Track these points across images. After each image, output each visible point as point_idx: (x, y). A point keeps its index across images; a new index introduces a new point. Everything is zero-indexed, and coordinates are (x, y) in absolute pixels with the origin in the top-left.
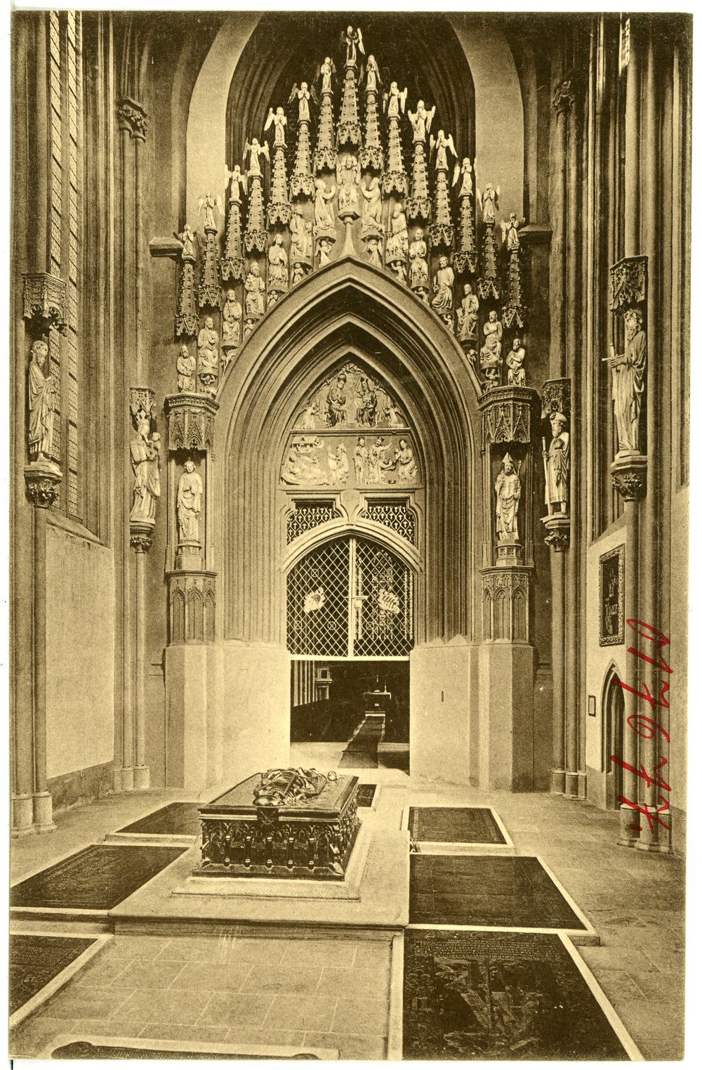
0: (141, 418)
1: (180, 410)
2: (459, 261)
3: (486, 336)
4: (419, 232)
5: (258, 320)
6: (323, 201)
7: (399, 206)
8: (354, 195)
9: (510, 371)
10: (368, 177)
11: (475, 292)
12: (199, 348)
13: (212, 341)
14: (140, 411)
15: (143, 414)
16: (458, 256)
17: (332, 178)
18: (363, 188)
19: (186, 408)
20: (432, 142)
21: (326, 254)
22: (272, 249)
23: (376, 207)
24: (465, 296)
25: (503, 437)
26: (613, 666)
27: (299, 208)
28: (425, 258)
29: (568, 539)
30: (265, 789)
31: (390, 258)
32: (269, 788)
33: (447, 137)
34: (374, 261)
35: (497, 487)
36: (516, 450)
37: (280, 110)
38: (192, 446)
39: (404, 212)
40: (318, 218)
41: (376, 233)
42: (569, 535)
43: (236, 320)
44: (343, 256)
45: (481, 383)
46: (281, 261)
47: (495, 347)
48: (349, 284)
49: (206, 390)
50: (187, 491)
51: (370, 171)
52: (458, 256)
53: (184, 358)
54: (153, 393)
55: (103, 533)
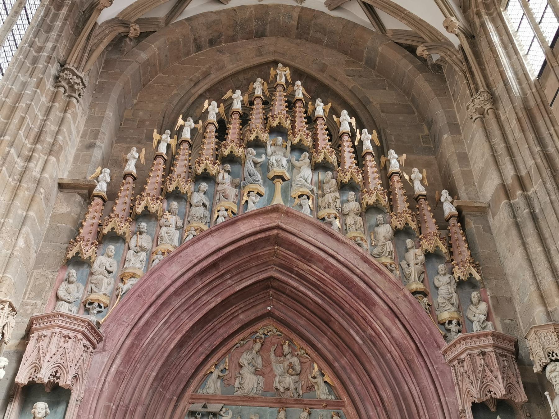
8: (284, 161)
11: (419, 246)
12: (92, 274)
13: (110, 269)
17: (262, 150)
22: (196, 194)
23: (307, 172)
24: (407, 250)
27: (228, 167)
31: (323, 213)
34: (306, 211)
40: (246, 174)
44: (275, 203)
46: (204, 205)
48: (275, 232)
51: (298, 148)
53: (70, 282)
54: (13, 310)
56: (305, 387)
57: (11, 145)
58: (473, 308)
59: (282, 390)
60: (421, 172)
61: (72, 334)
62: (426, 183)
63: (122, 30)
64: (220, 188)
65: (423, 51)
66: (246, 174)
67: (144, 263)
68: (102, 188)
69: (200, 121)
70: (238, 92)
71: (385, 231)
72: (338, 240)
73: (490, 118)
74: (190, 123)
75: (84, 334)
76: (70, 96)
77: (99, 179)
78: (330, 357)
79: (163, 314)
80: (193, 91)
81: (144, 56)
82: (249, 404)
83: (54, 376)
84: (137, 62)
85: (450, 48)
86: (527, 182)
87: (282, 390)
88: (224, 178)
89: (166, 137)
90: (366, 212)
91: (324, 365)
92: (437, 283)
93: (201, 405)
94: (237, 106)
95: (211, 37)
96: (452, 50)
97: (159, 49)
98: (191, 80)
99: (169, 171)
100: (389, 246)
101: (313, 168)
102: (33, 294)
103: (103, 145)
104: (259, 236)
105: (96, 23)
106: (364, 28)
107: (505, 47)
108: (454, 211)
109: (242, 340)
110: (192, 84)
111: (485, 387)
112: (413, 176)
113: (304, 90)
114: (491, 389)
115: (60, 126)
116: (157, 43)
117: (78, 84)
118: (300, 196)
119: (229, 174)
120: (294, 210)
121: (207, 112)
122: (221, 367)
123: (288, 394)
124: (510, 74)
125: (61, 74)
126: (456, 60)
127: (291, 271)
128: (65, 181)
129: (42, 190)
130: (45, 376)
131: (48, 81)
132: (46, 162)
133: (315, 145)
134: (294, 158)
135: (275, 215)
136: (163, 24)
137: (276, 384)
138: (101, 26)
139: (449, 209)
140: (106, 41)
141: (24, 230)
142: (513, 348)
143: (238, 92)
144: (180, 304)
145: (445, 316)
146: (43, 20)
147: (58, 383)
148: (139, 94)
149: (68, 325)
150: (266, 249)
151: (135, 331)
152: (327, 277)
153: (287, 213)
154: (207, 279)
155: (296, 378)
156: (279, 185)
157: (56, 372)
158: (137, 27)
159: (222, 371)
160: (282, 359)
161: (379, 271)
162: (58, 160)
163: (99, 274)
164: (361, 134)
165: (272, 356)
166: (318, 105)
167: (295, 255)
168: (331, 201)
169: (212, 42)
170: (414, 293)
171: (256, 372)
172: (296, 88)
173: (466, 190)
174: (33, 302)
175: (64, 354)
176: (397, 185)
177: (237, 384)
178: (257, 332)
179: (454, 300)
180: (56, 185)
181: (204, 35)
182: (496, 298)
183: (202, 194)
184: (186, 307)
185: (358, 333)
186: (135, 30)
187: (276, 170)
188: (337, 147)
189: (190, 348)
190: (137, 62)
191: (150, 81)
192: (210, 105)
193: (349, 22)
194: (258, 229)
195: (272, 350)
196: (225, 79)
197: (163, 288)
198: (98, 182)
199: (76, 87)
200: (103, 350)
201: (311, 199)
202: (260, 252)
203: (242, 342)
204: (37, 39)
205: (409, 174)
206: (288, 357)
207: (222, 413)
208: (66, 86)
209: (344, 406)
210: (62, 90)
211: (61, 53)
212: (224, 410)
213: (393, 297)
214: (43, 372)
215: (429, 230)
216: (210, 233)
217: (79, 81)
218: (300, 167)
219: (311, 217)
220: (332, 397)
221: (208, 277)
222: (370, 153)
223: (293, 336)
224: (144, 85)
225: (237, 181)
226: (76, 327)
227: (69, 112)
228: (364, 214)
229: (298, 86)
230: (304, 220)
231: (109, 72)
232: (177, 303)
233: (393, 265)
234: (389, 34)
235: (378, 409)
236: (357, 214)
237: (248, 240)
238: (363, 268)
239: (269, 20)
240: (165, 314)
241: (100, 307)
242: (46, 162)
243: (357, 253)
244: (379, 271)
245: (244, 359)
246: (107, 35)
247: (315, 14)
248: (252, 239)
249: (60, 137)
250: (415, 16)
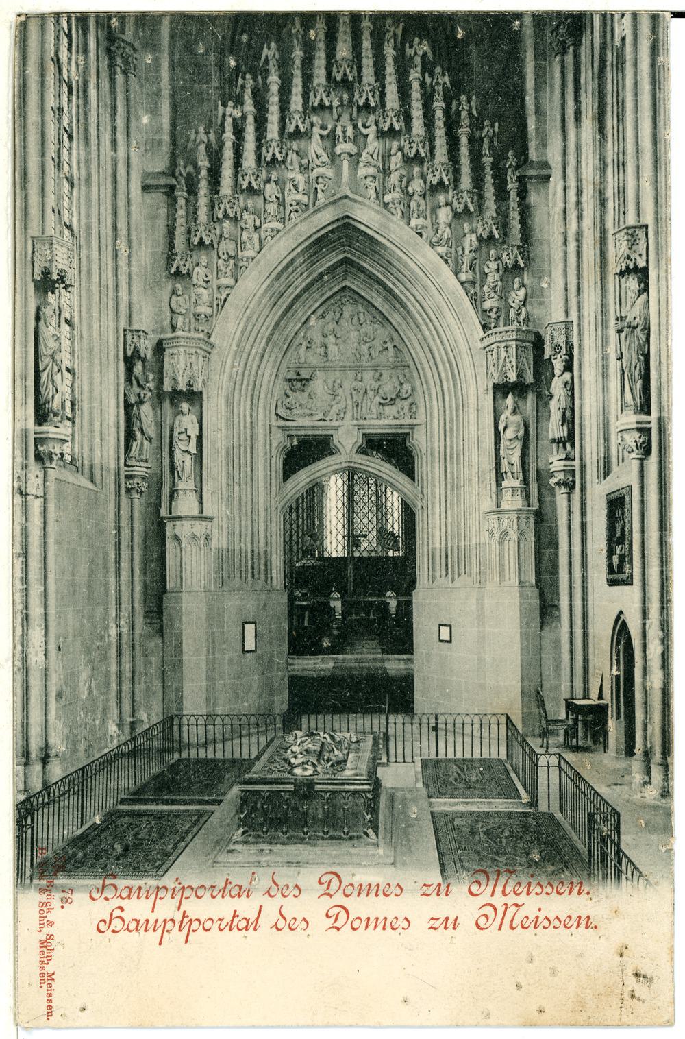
1: (175, 351)
2: (458, 199)
3: (487, 274)
6: (318, 137)
9: (512, 310)
10: (363, 114)
13: (206, 279)
16: (457, 194)
18: (360, 125)
20: (428, 80)
21: (323, 191)
25: (506, 377)
26: (621, 612)
27: (295, 145)
29: (574, 482)
30: (296, 757)
32: (300, 756)
33: (444, 75)
35: (501, 428)
36: (519, 389)
37: (273, 45)
38: (188, 387)
39: (401, 149)
42: (574, 476)
45: (483, 323)
47: (496, 286)
49: (201, 328)
50: (182, 433)
52: (457, 194)
53: (178, 296)
55: (98, 480)
92: (487, 270)
100: (447, 233)
130: (182, 386)
133: (383, 103)
145: (488, 304)
157: (190, 382)
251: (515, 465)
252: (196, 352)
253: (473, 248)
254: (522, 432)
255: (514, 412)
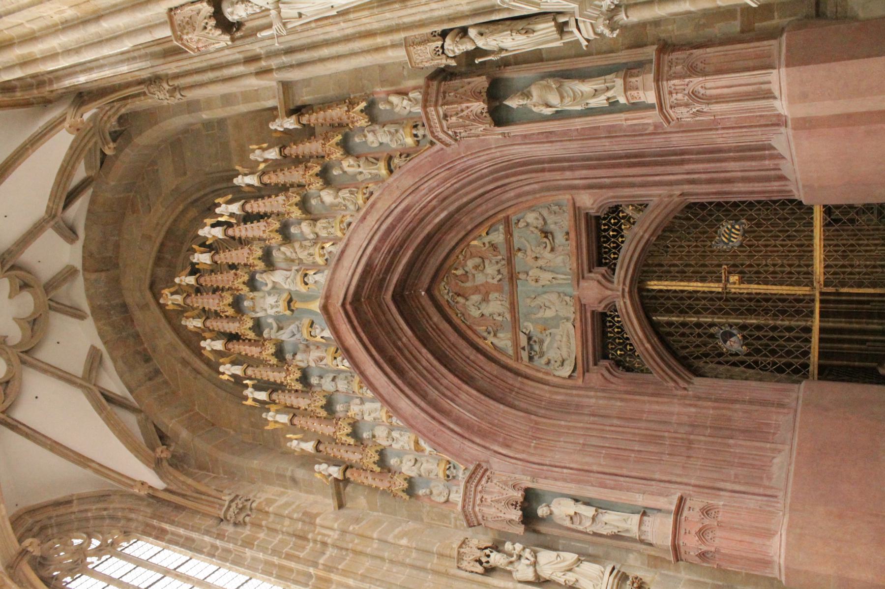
0: (488, 562)
4: (293, 230)
5: (387, 412)
6: (281, 332)
7: (275, 253)
8: (271, 300)
11: (340, 162)
13: (413, 461)
14: (481, 563)
15: (484, 559)
17: (263, 320)
19: (477, 509)
23: (278, 277)
25: (482, 113)
27: (288, 356)
28: (315, 220)
31: (320, 261)
38: (518, 508)
41: (299, 278)
43: (389, 433)
44: (319, 311)
46: (334, 379)
48: (348, 307)
51: (252, 285)
53: (431, 493)
54: (464, 542)
56: (495, 253)
57: (315, 564)
58: (397, 110)
59: (500, 276)
60: (253, 151)
61: (479, 497)
62: (265, 145)
63: (165, 464)
64: (312, 364)
65: (109, 148)
66: (292, 339)
67: (402, 433)
68: (335, 472)
69: (245, 382)
70: (203, 344)
71: (328, 196)
72: (346, 245)
73: (176, 83)
74: (249, 392)
75: (476, 486)
76: (251, 509)
77: (326, 474)
78: (463, 233)
79: (447, 406)
80: (206, 375)
81: (184, 434)
82: (516, 307)
83: (516, 506)
84: (193, 440)
85: (99, 119)
86: (249, 54)
87: (500, 276)
88: (301, 359)
89: (270, 416)
90: (310, 213)
91: (471, 237)
93: (522, 352)
94: (219, 345)
95: (143, 363)
96: (101, 115)
97: (172, 418)
98: (195, 378)
99: (306, 413)
100: (344, 193)
101: (271, 269)
102: (445, 520)
103: (290, 469)
104: (356, 323)
105: (166, 490)
106: (93, 201)
107: (91, 69)
108: (293, 119)
109: (457, 315)
110: (199, 376)
111: (478, 118)
112: (260, 160)
113: (183, 272)
114: (479, 111)
115: (285, 517)
116: (166, 421)
117: (237, 504)
118: (306, 284)
119: (296, 354)
120: (322, 292)
121: (233, 376)
122: (485, 334)
123: (505, 271)
124: (124, 68)
125: (232, 521)
126: (113, 110)
127: (384, 279)
128: (336, 504)
129: (351, 528)
130: (516, 514)
131: (243, 533)
132: (323, 527)
134: (265, 289)
135: (331, 310)
136: (143, 415)
137: (495, 282)
138: (168, 484)
139: (290, 123)
140: (182, 478)
141: (392, 541)
142: (435, 83)
143: (203, 344)
144: (434, 390)
145: (410, 141)
146: (182, 546)
147: (521, 502)
148: (224, 428)
149: (472, 500)
150: (366, 311)
151: (466, 435)
152: (385, 248)
153: (327, 297)
154: (406, 366)
155: (487, 262)
156: (297, 305)
157: (512, 505)
158: (159, 450)
159: (489, 333)
160: (470, 276)
161: (372, 206)
162: (318, 514)
163: (420, 471)
164: (222, 215)
165: (469, 284)
166: (198, 260)
167: (368, 281)
168: (306, 253)
169: (147, 360)
170: (391, 171)
171: (486, 300)
172: (183, 283)
173: (264, 100)
174: (453, 520)
175: (498, 501)
176: (272, 179)
177: (500, 318)
178: (447, 301)
179: (393, 130)
180: (341, 510)
181: (142, 371)
182: (383, 83)
183: (323, 381)
184: (435, 382)
185: (437, 215)
186: (162, 452)
187: (282, 308)
188: (242, 242)
189: (473, 370)
190: (193, 440)
191: (206, 419)
192: (223, 374)
193: (87, 219)
194: (349, 327)
195: (463, 285)
196: (184, 342)
197: (423, 415)
198: (330, 475)
199: (240, 506)
200: (488, 462)
201: (307, 272)
202: (370, 315)
203: (459, 315)
204: (205, 550)
205: (258, 163)
206: (467, 269)
207: (527, 332)
208: (243, 515)
209: (508, 217)
210: (247, 519)
211: (210, 522)
212: (524, 331)
213: (398, 193)
214: (513, 517)
215: (320, 150)
216: (362, 373)
217: (234, 505)
218: (274, 282)
219: (327, 272)
220: (501, 228)
221: (404, 366)
222: (243, 205)
223: (446, 266)
224: (213, 425)
225: (301, 347)
226: (472, 493)
227: (267, 509)
228: (312, 217)
229: (181, 281)
230: (331, 280)
231: (210, 466)
232: (433, 394)
233: (365, 191)
234: (92, 173)
235: (507, 189)
236: (315, 226)
237: (362, 335)
238: (371, 221)
239: (106, 303)
240: (446, 404)
241: (450, 467)
242: (323, 527)
243: (357, 226)
244: (372, 206)
245: (475, 313)
246: (174, 476)
247: (88, 255)
248: (359, 330)
249: (295, 516)
250: (67, 154)
251: (595, 87)
252: (480, 492)
253: (355, 164)
254: (552, 83)
255: (528, 95)
